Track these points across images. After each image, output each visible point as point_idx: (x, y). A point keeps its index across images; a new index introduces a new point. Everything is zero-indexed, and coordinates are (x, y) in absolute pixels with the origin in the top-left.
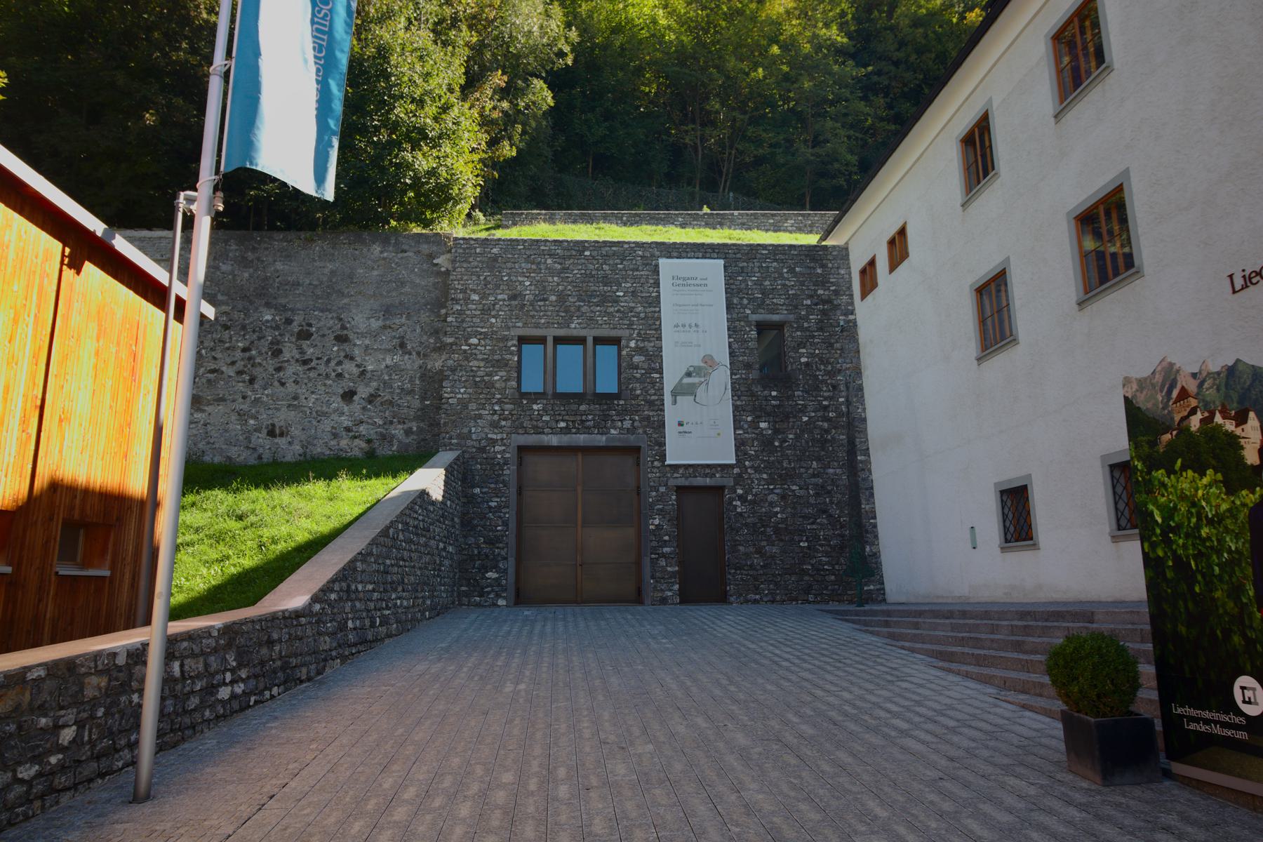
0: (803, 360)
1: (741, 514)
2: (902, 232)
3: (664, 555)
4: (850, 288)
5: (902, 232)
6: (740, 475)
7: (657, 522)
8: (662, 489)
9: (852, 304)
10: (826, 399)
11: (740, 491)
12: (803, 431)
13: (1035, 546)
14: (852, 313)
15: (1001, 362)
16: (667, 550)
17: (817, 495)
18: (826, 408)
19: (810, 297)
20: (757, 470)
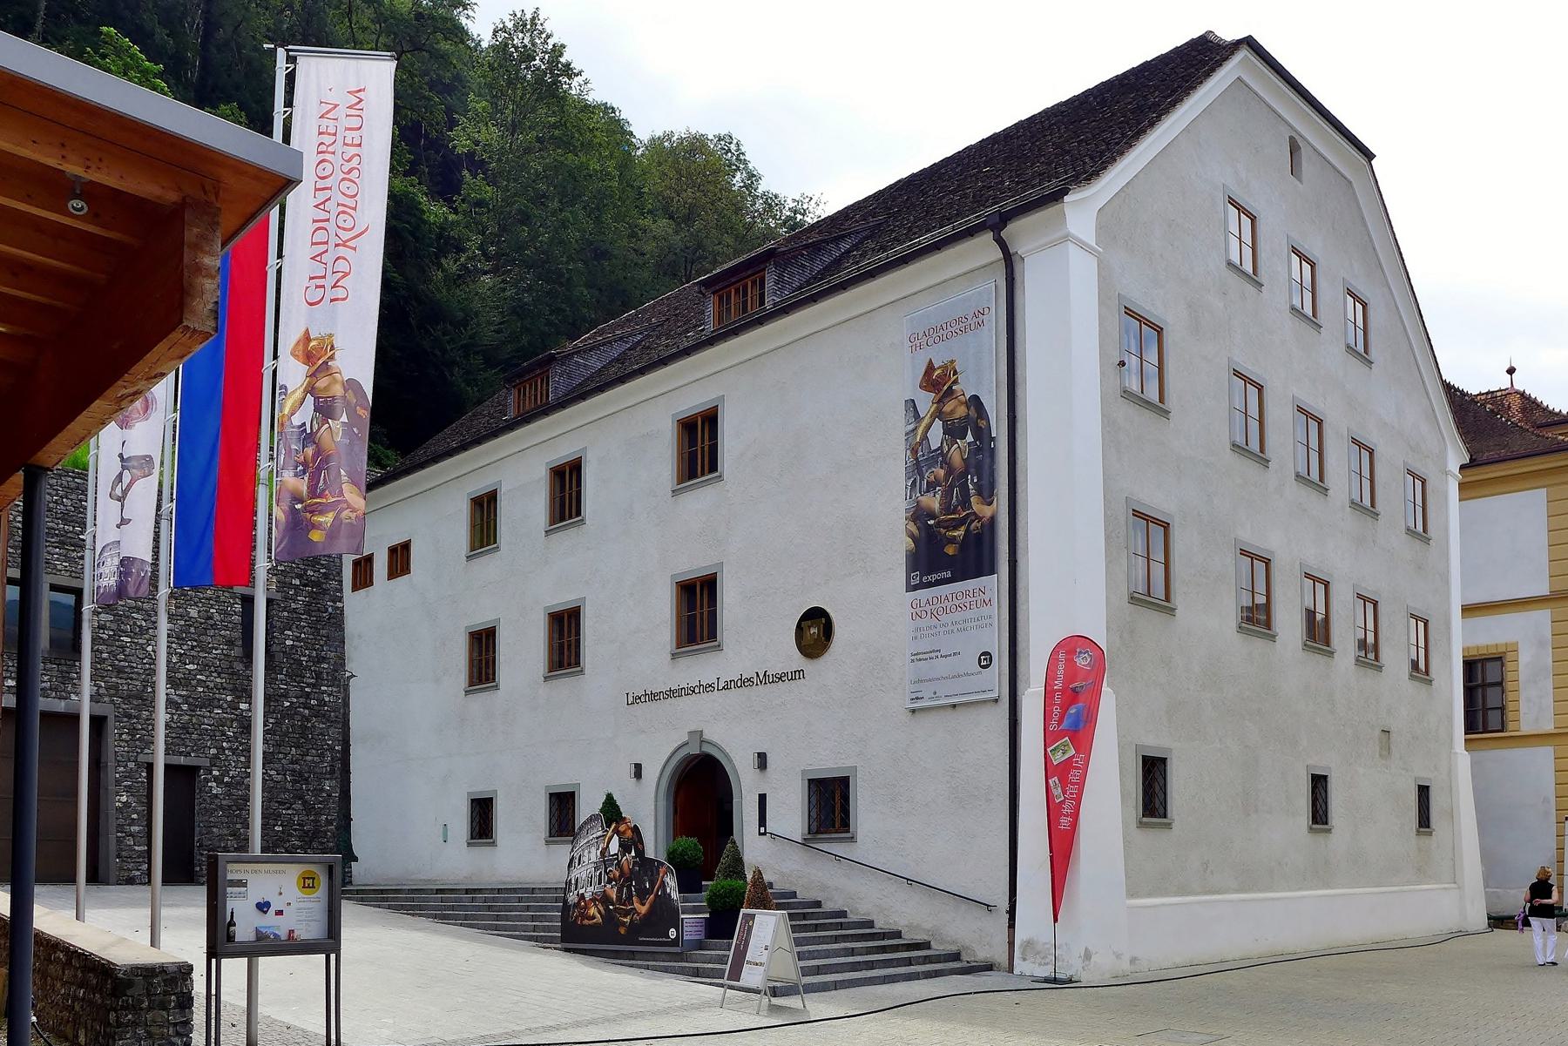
0: (289, 643)
1: (216, 796)
2: (406, 546)
3: (131, 835)
4: (340, 573)
5: (406, 546)
6: (216, 757)
7: (124, 799)
8: (131, 765)
9: (341, 590)
10: (308, 685)
11: (216, 773)
12: (283, 717)
13: (494, 844)
14: (341, 599)
15: (482, 700)
16: (135, 829)
17: (294, 782)
18: (308, 695)
19: (299, 576)
20: (234, 751)
